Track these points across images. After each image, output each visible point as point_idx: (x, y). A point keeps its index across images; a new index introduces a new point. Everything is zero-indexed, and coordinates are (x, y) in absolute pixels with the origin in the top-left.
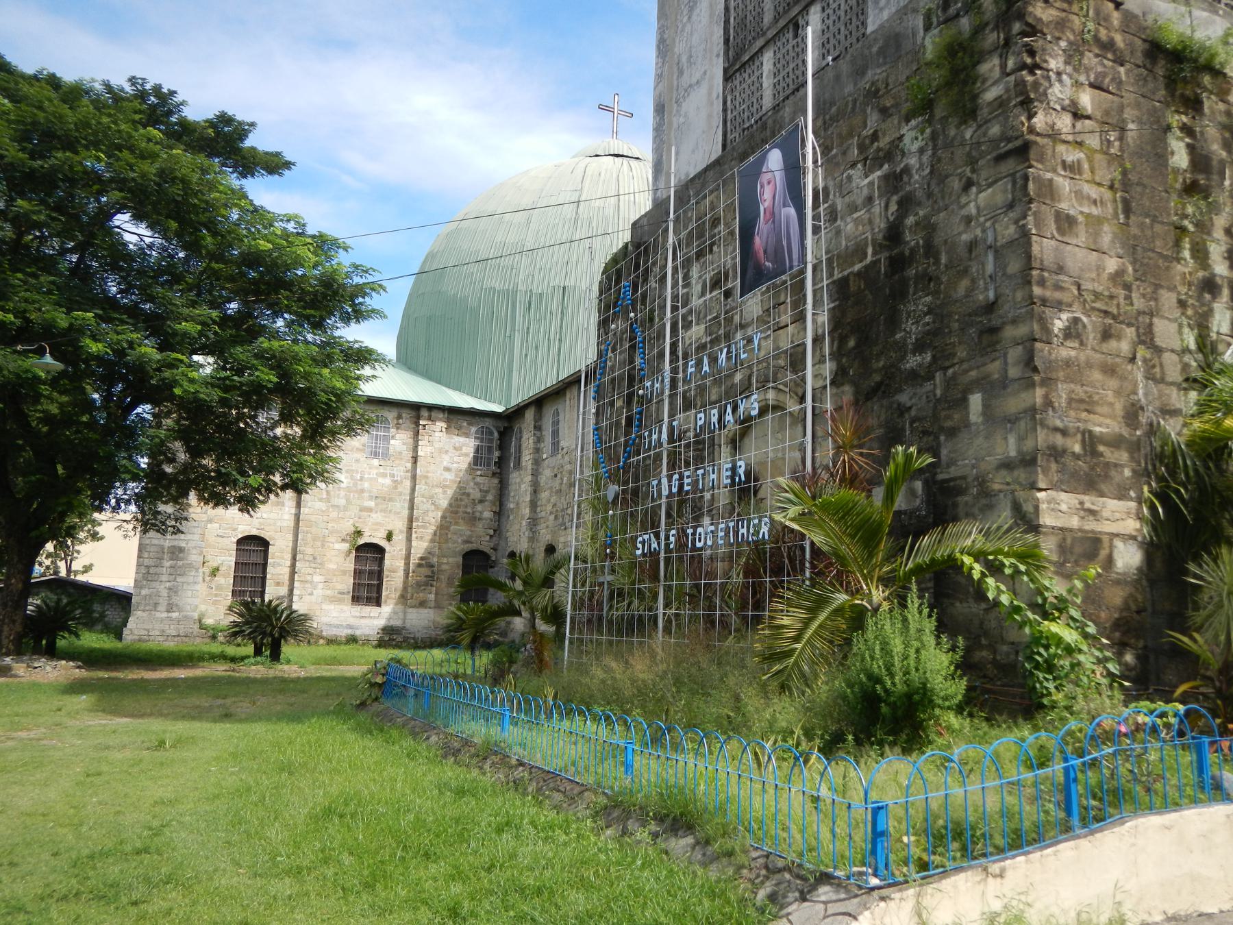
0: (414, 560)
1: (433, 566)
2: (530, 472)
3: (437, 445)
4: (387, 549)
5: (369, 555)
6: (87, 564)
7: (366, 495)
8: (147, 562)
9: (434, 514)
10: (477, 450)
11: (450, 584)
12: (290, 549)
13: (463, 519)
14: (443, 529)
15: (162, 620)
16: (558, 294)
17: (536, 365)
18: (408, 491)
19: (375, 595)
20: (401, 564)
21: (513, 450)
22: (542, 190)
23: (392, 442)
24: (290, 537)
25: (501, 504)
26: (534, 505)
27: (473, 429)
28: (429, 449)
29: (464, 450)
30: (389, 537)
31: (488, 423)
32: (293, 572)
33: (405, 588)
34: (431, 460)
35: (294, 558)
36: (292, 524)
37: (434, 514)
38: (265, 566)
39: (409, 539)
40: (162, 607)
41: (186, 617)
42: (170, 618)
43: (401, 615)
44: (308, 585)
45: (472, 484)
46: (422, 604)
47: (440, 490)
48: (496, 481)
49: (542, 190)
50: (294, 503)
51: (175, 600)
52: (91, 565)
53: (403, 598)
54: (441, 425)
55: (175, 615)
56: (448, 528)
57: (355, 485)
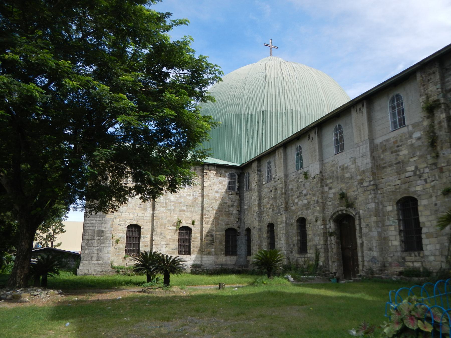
0: (205, 233)
1: (213, 236)
2: (256, 190)
3: (212, 181)
4: (193, 229)
5: (185, 231)
6: (59, 242)
7: (182, 204)
8: (87, 238)
9: (212, 212)
10: (229, 183)
11: (221, 243)
12: (150, 230)
13: (225, 214)
14: (216, 218)
15: (94, 265)
16: (260, 115)
17: (252, 145)
18: (200, 202)
19: (188, 250)
20: (199, 235)
21: (245, 182)
24: (150, 224)
25: (241, 207)
26: (259, 205)
27: (227, 174)
28: (209, 183)
29: (224, 183)
30: (193, 223)
31: (233, 171)
32: (152, 240)
33: (201, 246)
34: (210, 188)
35: (152, 234)
36: (151, 218)
37: (212, 212)
38: (139, 238)
39: (202, 224)
40: (95, 258)
41: (105, 263)
42: (98, 264)
43: (200, 259)
44: (159, 246)
45: (228, 198)
46: (209, 254)
47: (215, 201)
48: (238, 197)
50: (152, 209)
51: (100, 255)
52: (61, 243)
53: (201, 251)
54: (213, 172)
55: (100, 262)
56: (218, 218)
57: (177, 200)
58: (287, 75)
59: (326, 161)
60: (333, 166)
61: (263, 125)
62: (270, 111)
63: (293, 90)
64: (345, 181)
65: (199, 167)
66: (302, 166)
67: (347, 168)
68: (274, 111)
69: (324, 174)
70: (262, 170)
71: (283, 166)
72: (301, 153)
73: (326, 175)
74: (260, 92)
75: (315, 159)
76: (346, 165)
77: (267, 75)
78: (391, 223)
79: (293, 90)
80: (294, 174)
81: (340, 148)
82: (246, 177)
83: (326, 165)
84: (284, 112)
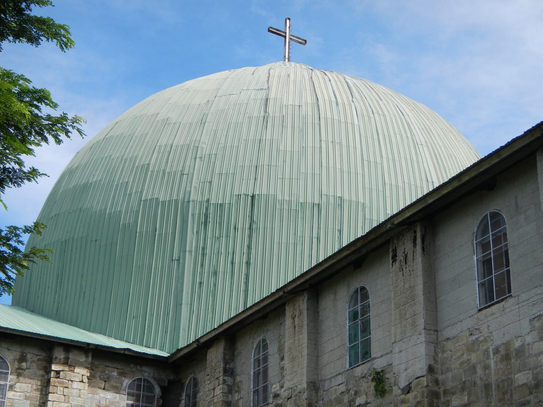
17: (214, 296)
22: (218, 89)
23: (10, 394)
27: (127, 382)
31: (147, 373)
49: (218, 89)
54: (82, 372)
58: (330, 101)
59: (449, 333)
60: (471, 348)
61: (250, 237)
62: (275, 196)
63: (344, 143)
64: (516, 397)
65: (36, 351)
66: (366, 354)
67: (520, 352)
68: (287, 198)
69: (440, 377)
70: (238, 370)
71: (305, 352)
72: (366, 309)
73: (448, 379)
74: (247, 141)
75: (414, 325)
76: (517, 344)
77: (272, 95)
79: (344, 143)
80: (340, 379)
81: (496, 288)
82: (188, 396)
83: (449, 345)
84: (317, 202)
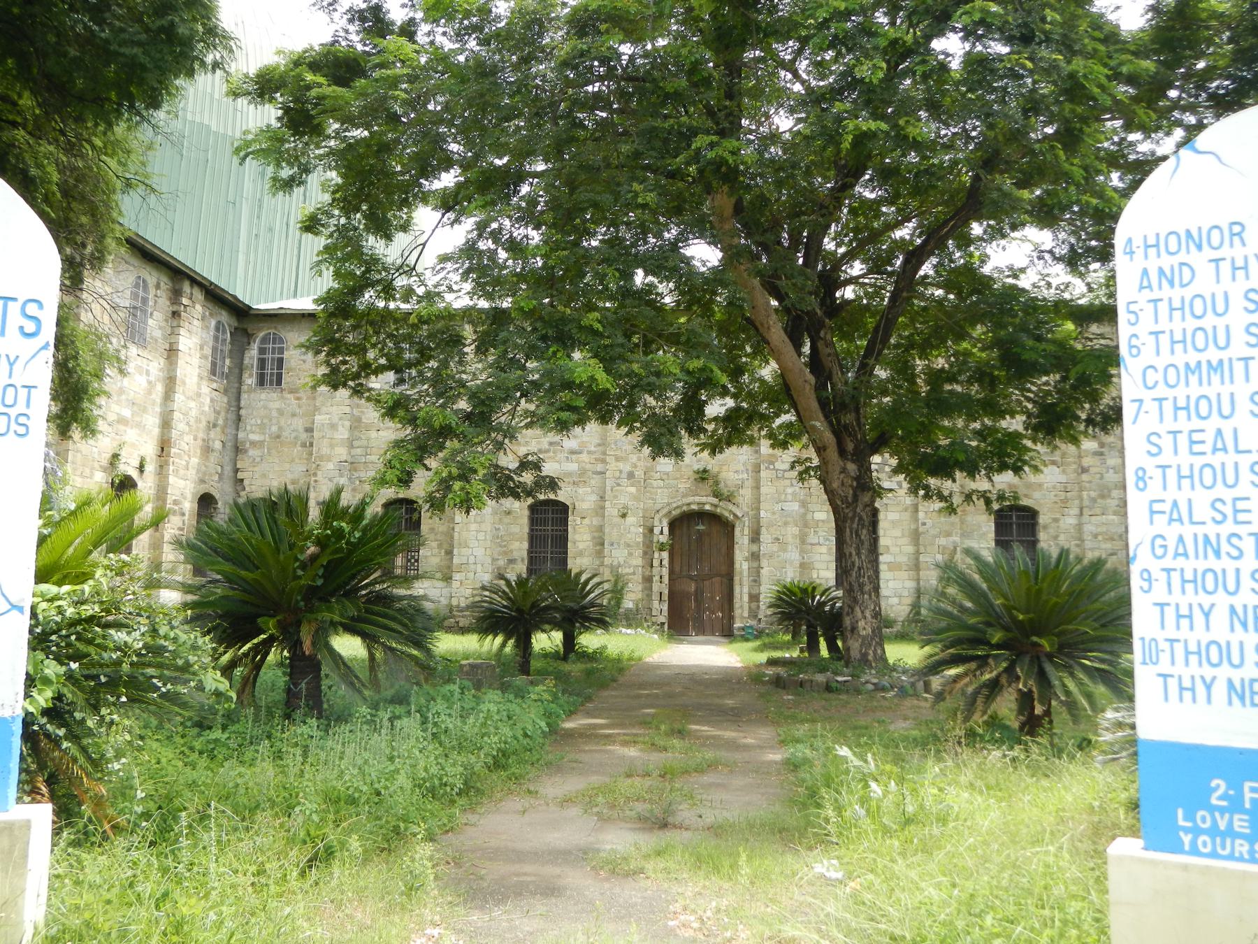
30: (141, 468)
78: (822, 541)
